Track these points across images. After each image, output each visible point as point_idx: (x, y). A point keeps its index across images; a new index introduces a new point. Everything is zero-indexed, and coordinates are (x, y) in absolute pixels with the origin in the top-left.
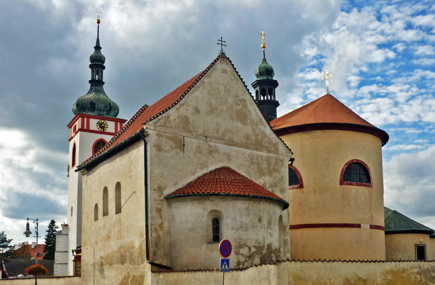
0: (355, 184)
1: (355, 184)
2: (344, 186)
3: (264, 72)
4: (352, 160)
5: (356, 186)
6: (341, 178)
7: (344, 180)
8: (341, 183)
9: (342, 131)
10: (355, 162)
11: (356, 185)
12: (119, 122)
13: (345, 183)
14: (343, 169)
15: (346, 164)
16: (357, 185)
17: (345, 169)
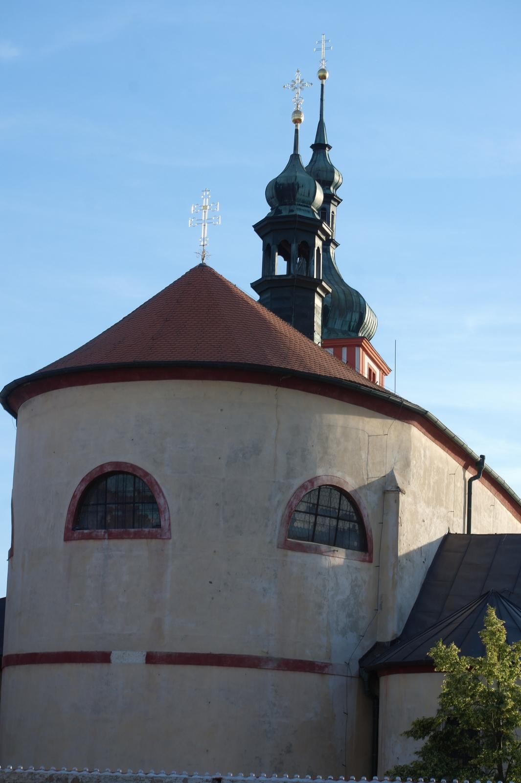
0: (104, 535)
1: (104, 535)
2: (74, 544)
3: (273, 197)
4: (102, 467)
5: (106, 541)
6: (68, 522)
7: (74, 529)
8: (67, 539)
9: (80, 388)
10: (109, 469)
11: (106, 536)
12: (344, 346)
13: (75, 535)
14: (74, 496)
15: (83, 480)
16: (109, 539)
17: (78, 497)
